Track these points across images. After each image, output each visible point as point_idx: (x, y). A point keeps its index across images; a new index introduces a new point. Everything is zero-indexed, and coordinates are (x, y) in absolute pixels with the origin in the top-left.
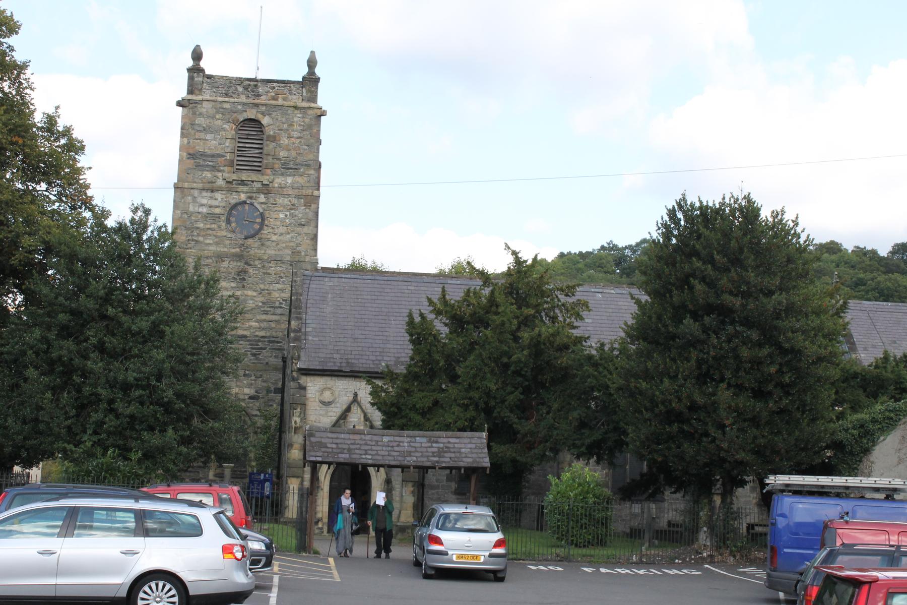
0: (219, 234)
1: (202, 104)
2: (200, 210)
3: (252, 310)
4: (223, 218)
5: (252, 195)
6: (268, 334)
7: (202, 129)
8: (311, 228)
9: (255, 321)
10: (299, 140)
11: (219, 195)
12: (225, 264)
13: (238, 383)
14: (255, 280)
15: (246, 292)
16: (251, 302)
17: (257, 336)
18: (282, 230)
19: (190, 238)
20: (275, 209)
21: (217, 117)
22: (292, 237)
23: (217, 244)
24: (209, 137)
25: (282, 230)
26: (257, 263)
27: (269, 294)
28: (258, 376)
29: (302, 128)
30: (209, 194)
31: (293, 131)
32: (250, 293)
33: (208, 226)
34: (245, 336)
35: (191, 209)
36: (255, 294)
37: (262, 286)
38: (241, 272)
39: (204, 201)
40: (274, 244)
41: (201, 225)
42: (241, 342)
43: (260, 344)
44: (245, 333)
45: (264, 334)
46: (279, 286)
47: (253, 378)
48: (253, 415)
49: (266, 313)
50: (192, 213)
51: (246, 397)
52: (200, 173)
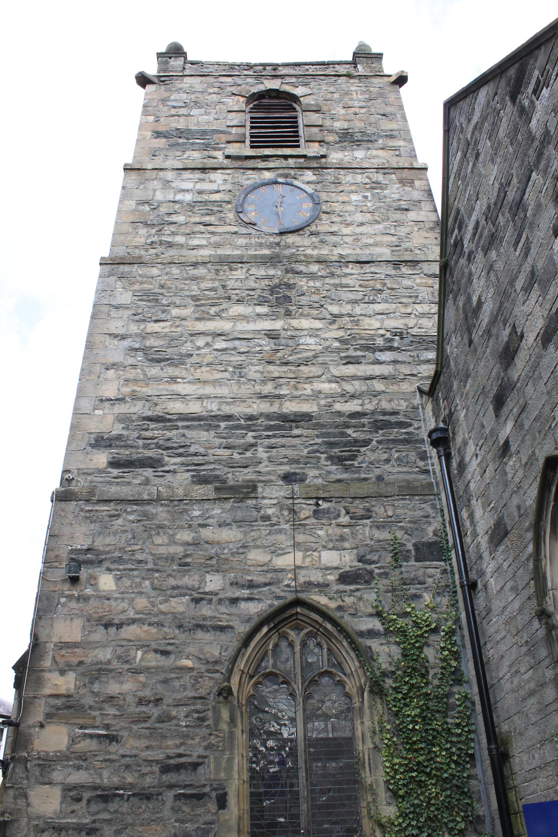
0: (220, 229)
1: (183, 80)
2: (179, 197)
3: (315, 357)
4: (229, 206)
5: (286, 171)
6: (369, 407)
7: (183, 105)
8: (423, 213)
9: (330, 382)
10: (363, 111)
11: (220, 175)
12: (240, 273)
13: (300, 538)
14: (315, 298)
15: (295, 323)
16: (312, 341)
17: (339, 414)
18: (359, 217)
19: (155, 239)
20: (341, 189)
21: (211, 91)
22: (385, 228)
23: (217, 245)
24: (195, 112)
25: (359, 217)
26: (314, 268)
27: (357, 323)
28: (360, 512)
29: (367, 96)
30: (198, 175)
31: (352, 99)
32: (305, 323)
33: (197, 220)
34: (306, 417)
35: (159, 196)
36: (318, 324)
37: (335, 309)
38: (278, 286)
39: (189, 185)
40: (348, 239)
41: (181, 219)
42: (296, 432)
43: (349, 431)
44: (305, 408)
45: (359, 409)
46: (378, 307)
47: (345, 519)
48: (361, 634)
49: (350, 361)
50: (160, 203)
51: (331, 578)
52: (179, 153)
